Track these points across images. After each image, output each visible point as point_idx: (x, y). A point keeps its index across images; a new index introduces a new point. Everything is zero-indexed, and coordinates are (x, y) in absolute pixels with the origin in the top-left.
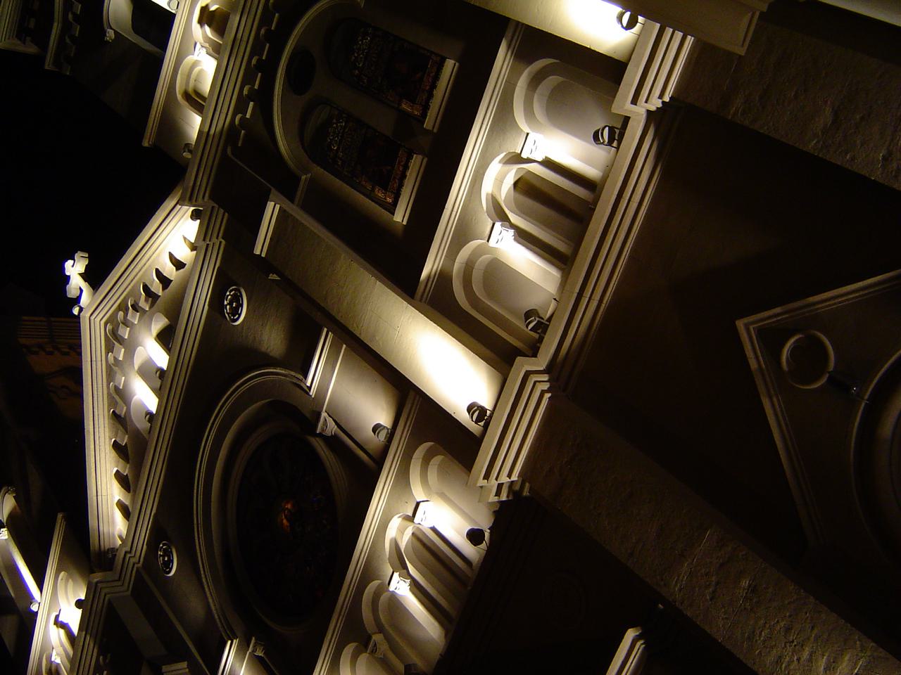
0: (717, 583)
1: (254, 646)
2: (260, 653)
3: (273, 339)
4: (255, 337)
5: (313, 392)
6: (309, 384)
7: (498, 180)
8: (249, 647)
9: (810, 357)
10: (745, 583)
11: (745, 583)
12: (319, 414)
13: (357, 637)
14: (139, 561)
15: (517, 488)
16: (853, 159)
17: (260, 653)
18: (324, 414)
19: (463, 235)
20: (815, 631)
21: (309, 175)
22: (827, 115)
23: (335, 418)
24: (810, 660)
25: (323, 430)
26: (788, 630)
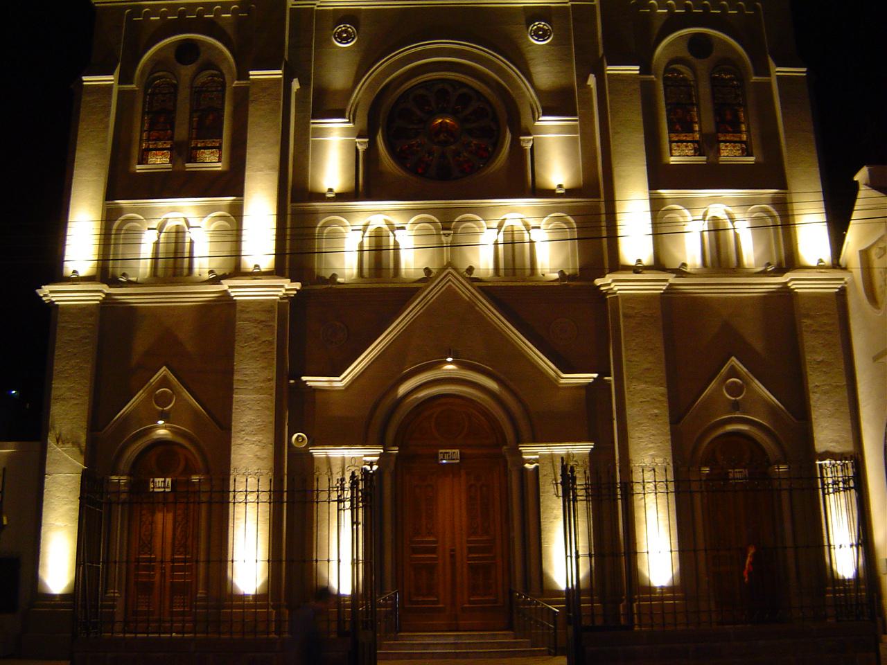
0: (648, 401)
1: (365, 143)
2: (360, 147)
3: (545, 75)
4: (533, 59)
5: (537, 123)
6: (540, 119)
7: (718, 210)
8: (358, 137)
9: (735, 390)
10: (656, 411)
11: (656, 411)
12: (529, 134)
13: (447, 222)
14: (318, 6)
15: (610, 292)
16: (811, 375)
17: (361, 148)
18: (532, 137)
19: (688, 204)
20: (660, 444)
21: (655, 79)
22: (820, 359)
23: (535, 145)
24: (650, 448)
25: (524, 140)
26: (653, 435)
